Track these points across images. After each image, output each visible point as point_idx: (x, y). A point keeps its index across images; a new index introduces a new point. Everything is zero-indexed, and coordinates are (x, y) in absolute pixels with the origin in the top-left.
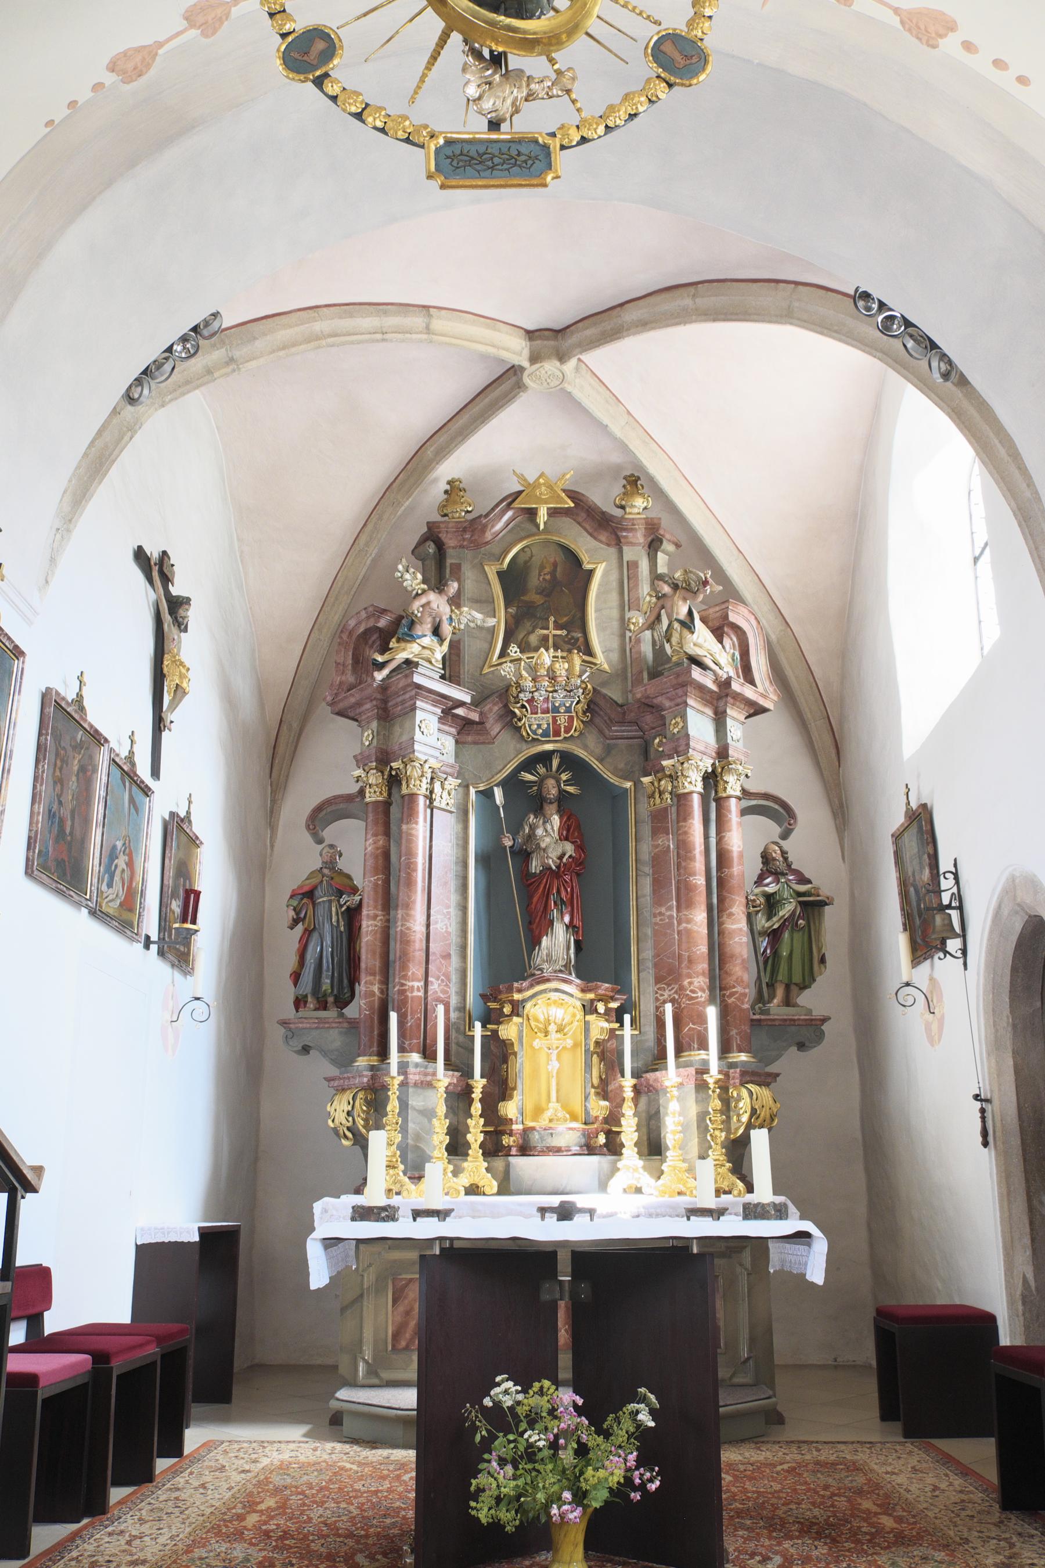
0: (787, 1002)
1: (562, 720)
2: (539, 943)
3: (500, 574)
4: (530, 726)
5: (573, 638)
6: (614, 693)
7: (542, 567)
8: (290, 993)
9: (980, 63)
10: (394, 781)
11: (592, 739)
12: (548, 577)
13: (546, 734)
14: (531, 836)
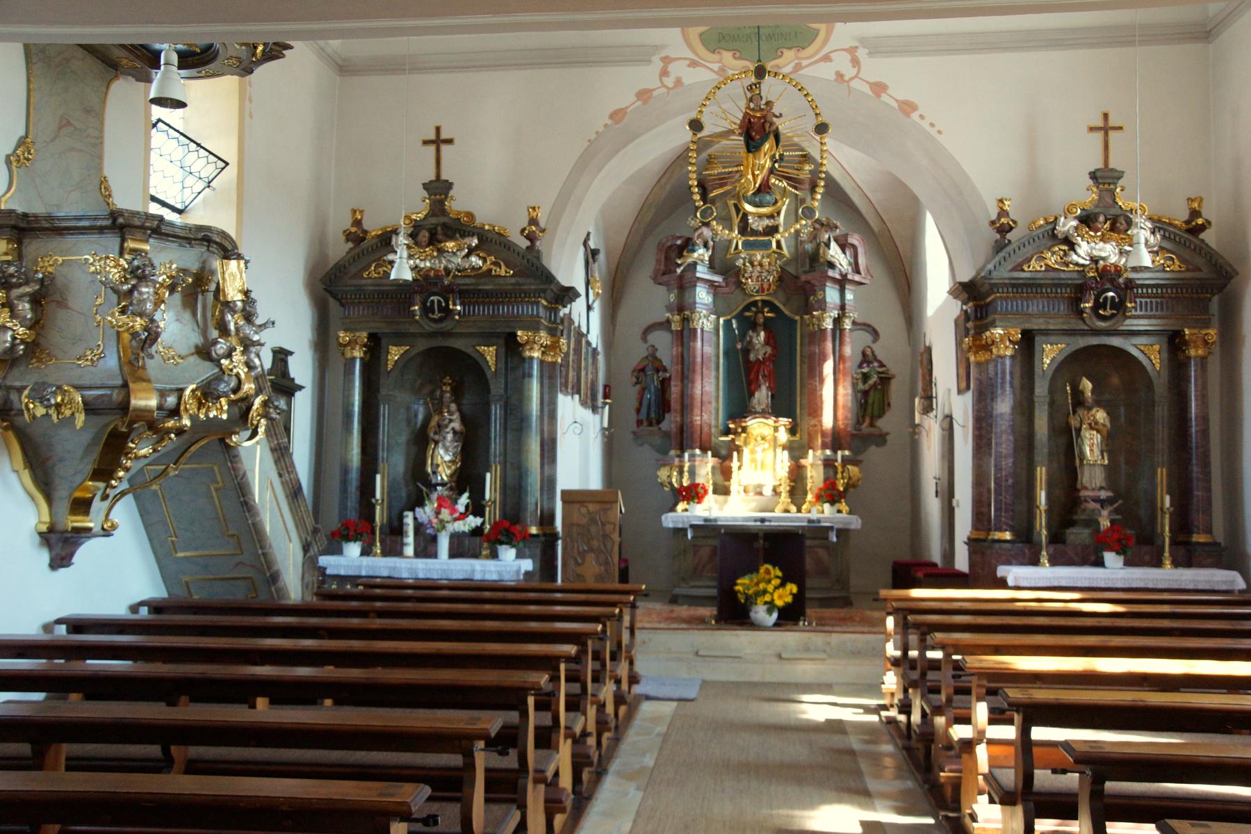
0: (872, 425)
1: (766, 286)
6: (791, 270)
8: (633, 417)
9: (925, 124)
10: (686, 320)
11: (781, 294)
14: (750, 342)
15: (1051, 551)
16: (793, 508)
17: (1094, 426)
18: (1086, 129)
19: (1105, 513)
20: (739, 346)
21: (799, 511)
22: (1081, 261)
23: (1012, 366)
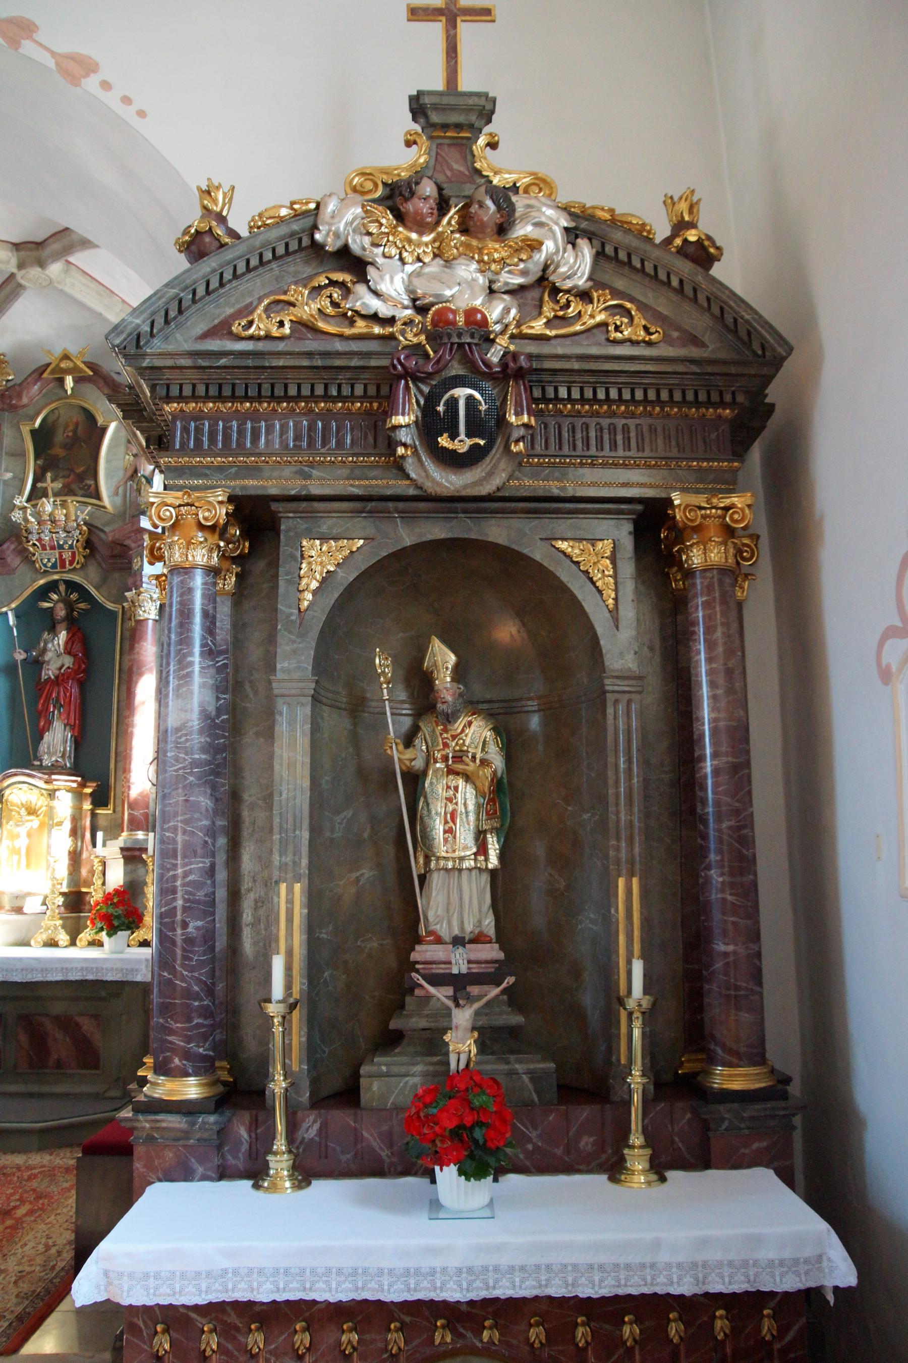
1: (67, 555)
2: (42, 738)
3: (34, 433)
4: (41, 560)
5: (86, 485)
7: (67, 426)
9: (112, 100)
12: (70, 434)
13: (54, 566)
15: (310, 1128)
16: (63, 937)
17: (458, 764)
18: (404, 13)
19: (463, 1017)
20: (20, 656)
21: (73, 943)
22: (384, 310)
23: (211, 597)
